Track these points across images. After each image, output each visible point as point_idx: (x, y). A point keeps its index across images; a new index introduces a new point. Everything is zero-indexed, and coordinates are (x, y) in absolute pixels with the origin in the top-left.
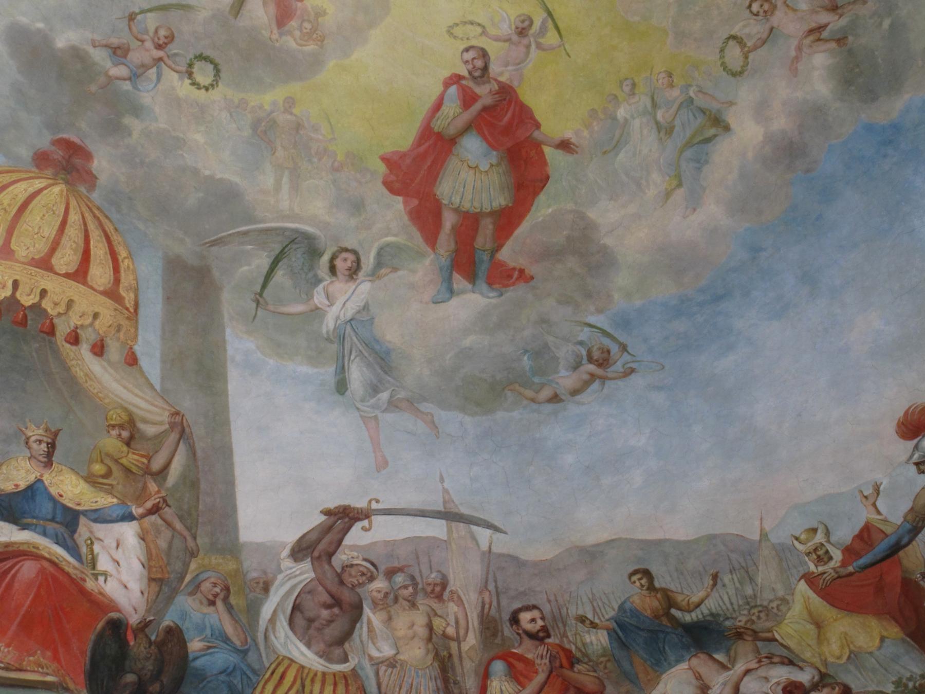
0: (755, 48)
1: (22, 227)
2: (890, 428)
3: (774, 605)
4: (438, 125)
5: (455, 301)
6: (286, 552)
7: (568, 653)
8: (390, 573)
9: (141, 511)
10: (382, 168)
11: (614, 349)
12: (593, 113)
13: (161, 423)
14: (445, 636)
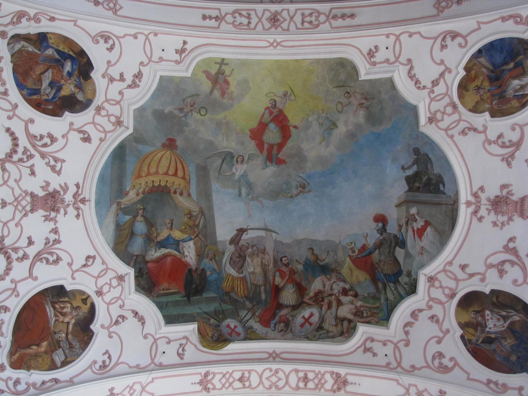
0: (345, 106)
1: (161, 165)
3: (341, 263)
4: (263, 121)
5: (267, 169)
6: (228, 243)
7: (293, 270)
8: (253, 246)
9: (194, 237)
10: (249, 133)
11: (306, 184)
13: (197, 211)
14: (265, 264)
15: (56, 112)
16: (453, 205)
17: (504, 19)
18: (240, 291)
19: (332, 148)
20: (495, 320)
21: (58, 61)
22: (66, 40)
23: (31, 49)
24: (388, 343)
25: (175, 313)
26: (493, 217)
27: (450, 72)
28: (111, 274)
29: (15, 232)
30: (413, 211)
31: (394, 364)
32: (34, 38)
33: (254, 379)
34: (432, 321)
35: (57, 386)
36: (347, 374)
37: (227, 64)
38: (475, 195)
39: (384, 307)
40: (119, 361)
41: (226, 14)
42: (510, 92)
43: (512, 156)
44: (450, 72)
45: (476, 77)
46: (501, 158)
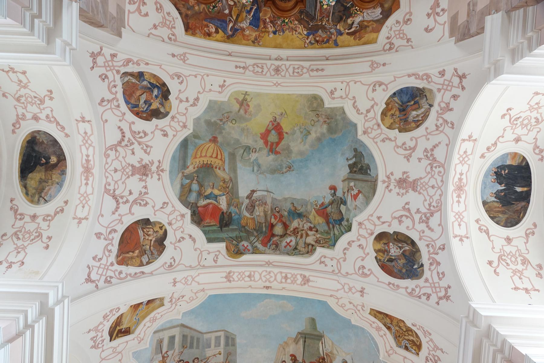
1: (208, 151)
2: (328, 187)
4: (268, 128)
8: (259, 201)
10: (260, 135)
12: (291, 128)
15: (147, 119)
16: (374, 182)
17: (409, 76)
18: (251, 226)
19: (307, 146)
20: (395, 248)
21: (149, 88)
22: (155, 76)
23: (134, 81)
24: (334, 259)
25: (213, 237)
26: (397, 190)
27: (377, 105)
28: (177, 213)
29: (122, 187)
30: (352, 184)
31: (337, 271)
32: (136, 75)
33: (257, 276)
34: (360, 248)
35: (143, 276)
36: (310, 276)
37: (249, 95)
38: (388, 177)
39: (333, 239)
40: (180, 263)
41: (249, 66)
42: (411, 118)
44: (377, 105)
45: (392, 109)
46: (404, 156)
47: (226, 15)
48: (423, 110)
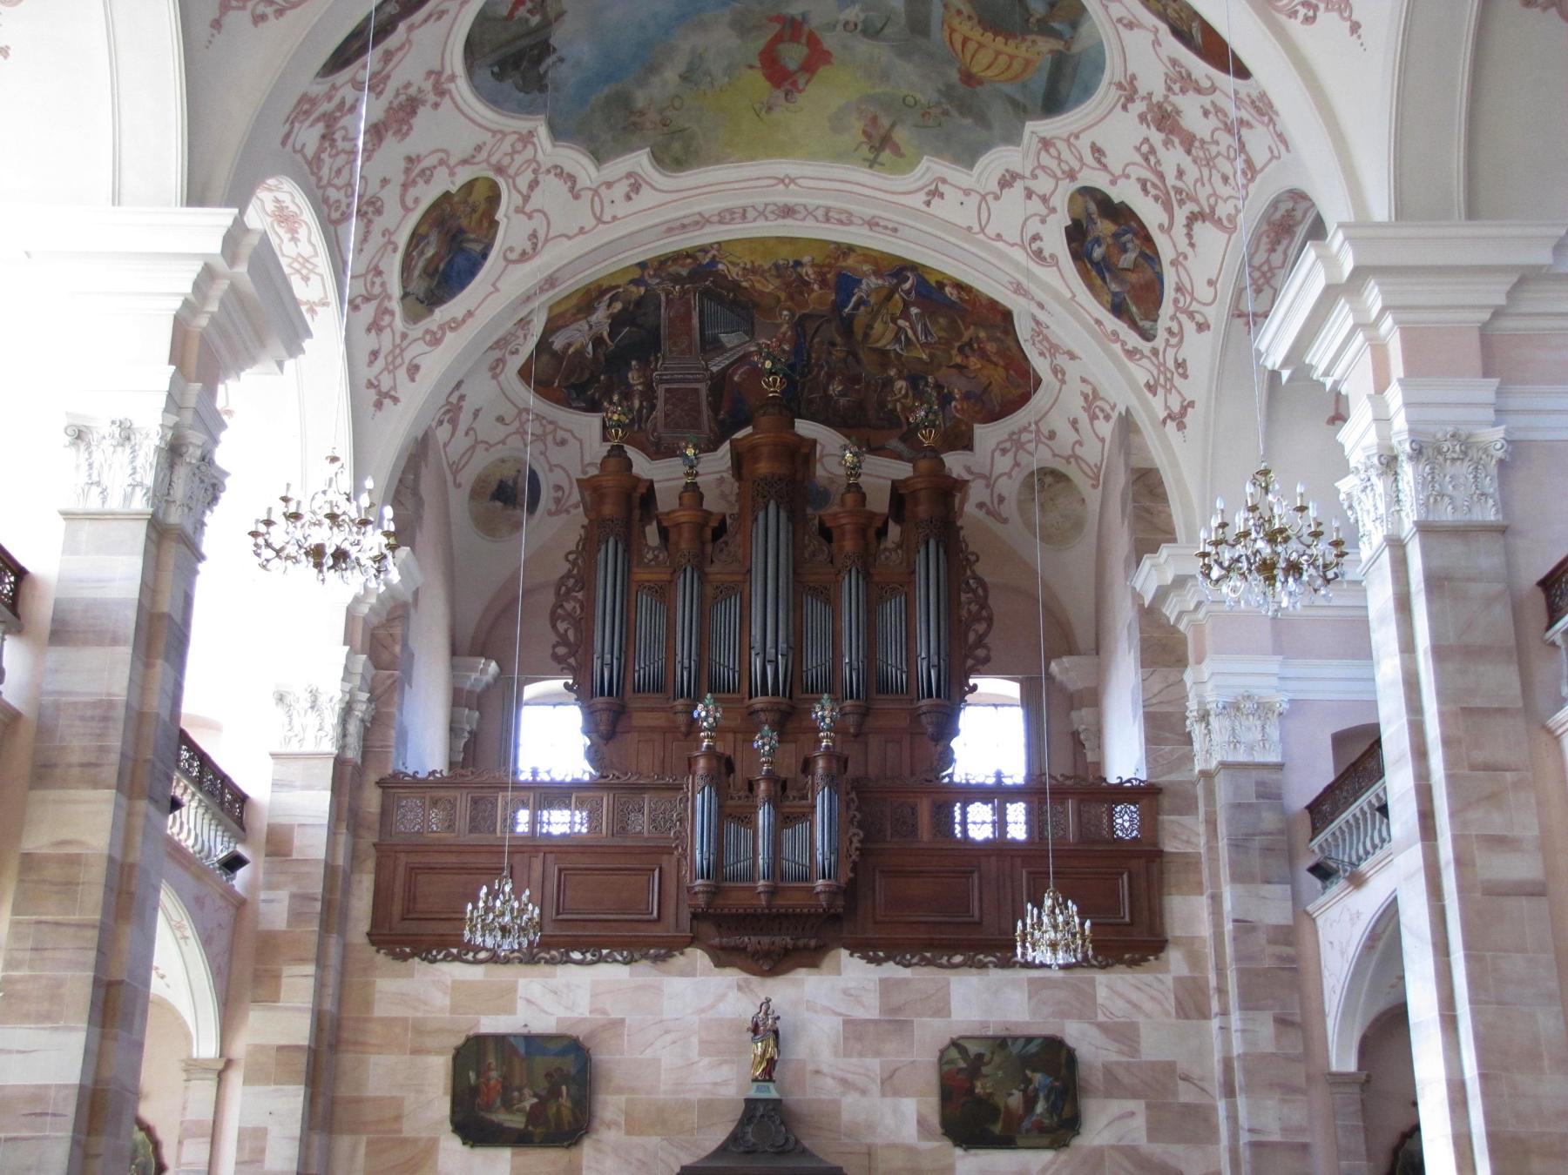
17: (470, 314)
21: (1108, 269)
22: (1091, 286)
23: (1134, 309)
26: (413, 91)
30: (535, 20)
38: (441, 93)
42: (434, 238)
43: (407, 171)
45: (481, 221)
47: (913, 304)
48: (416, 273)
